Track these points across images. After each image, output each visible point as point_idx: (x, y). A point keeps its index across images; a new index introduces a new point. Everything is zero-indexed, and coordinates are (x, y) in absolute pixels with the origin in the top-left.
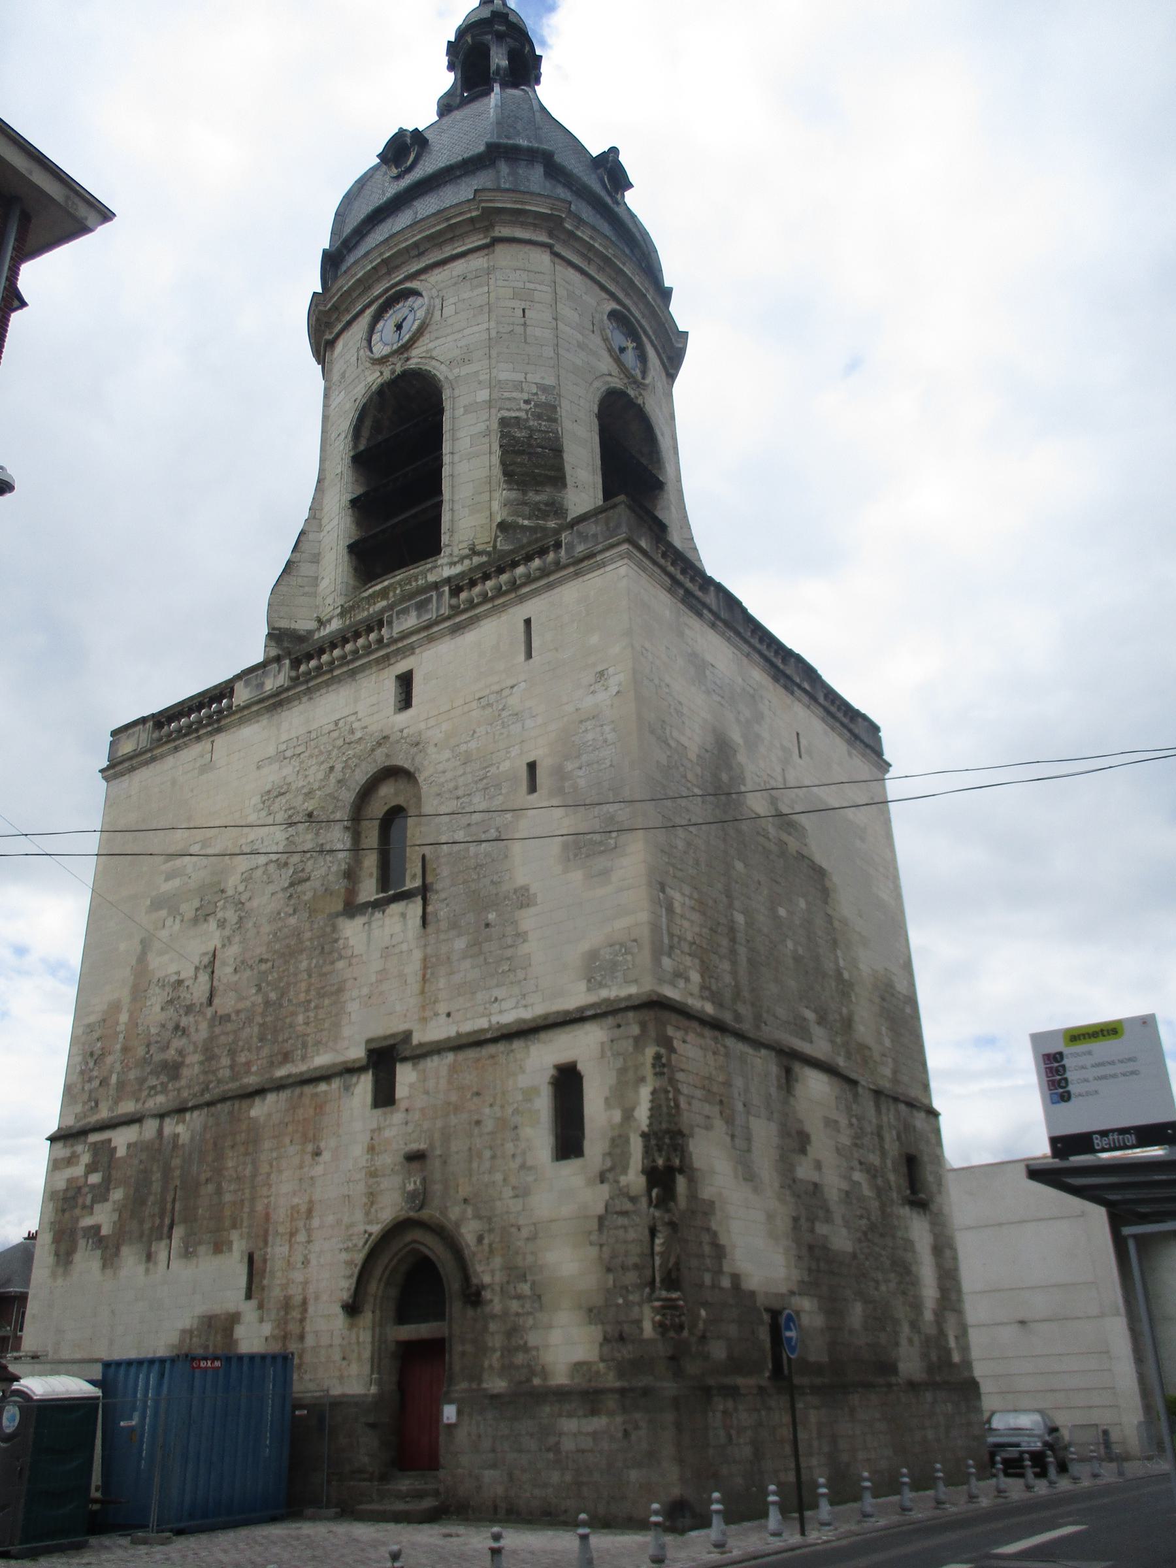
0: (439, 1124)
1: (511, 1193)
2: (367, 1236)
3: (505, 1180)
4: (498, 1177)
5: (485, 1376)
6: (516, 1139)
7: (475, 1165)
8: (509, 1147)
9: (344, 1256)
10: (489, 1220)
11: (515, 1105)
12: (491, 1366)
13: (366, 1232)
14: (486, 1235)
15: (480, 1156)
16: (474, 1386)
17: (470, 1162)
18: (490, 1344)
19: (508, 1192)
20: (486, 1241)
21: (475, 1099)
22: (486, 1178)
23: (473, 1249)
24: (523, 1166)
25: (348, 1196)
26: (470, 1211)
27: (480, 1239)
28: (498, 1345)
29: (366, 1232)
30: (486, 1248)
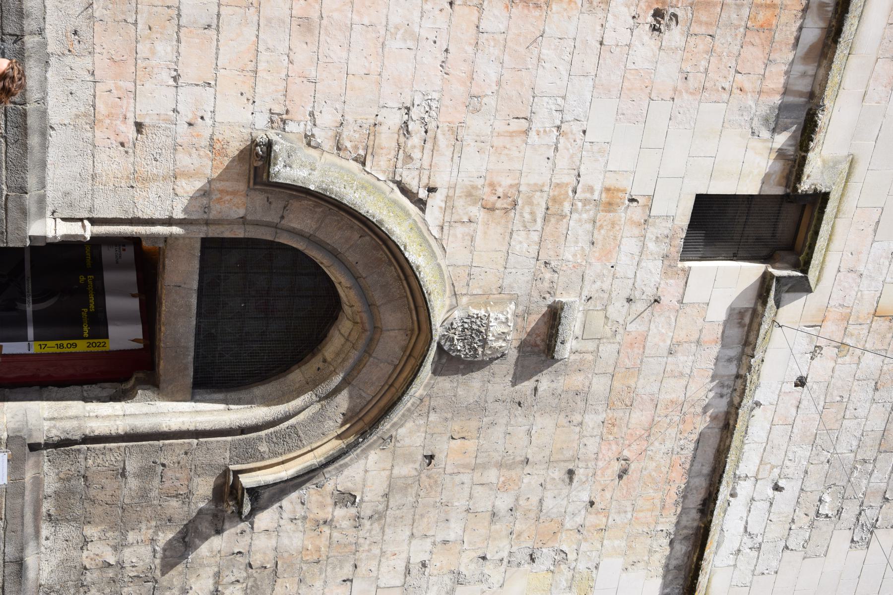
0: (600, 385)
1: (416, 560)
2: (423, 194)
3: (445, 542)
4: (454, 531)
5: (65, 530)
6: (510, 562)
7: (492, 475)
8: (500, 548)
9: (394, 119)
10: (378, 516)
11: (572, 556)
12: (86, 542)
13: (432, 190)
14: (353, 511)
15: (503, 488)
16: (47, 506)
17: (500, 466)
18: (131, 537)
19: (419, 551)
20: (340, 512)
21: (617, 467)
22: (461, 503)
23: (329, 486)
24: (458, 579)
25: (526, 132)
26: (405, 470)
27: (347, 498)
28: (128, 555)
29: (432, 190)
30: (327, 513)
